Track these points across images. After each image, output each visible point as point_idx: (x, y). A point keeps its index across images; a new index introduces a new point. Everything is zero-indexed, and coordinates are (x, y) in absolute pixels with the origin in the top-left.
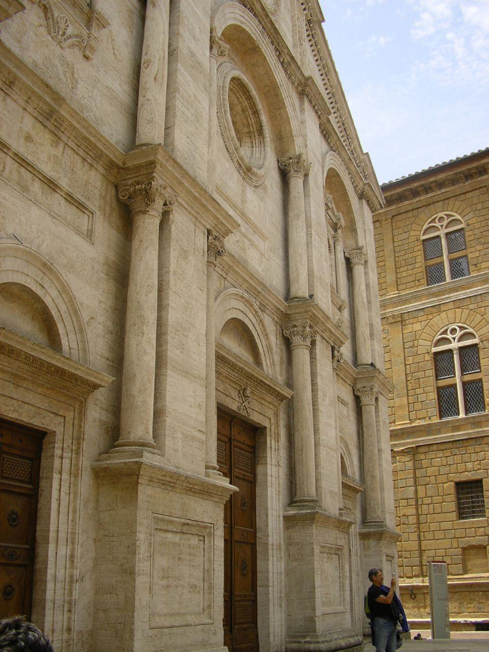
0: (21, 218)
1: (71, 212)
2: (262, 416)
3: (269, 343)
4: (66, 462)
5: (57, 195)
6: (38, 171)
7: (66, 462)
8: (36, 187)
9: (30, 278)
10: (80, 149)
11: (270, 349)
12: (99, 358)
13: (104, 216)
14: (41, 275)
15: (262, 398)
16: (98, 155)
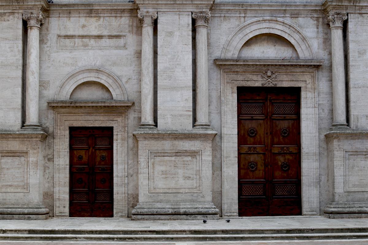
0: (85, 57)
1: (113, 42)
2: (294, 82)
3: (302, 36)
4: (119, 136)
5: (103, 39)
6: (91, 36)
7: (119, 136)
8: (92, 42)
9: (92, 77)
10: (112, 14)
11: (304, 39)
12: (134, 93)
13: (133, 34)
14: (97, 74)
15: (291, 72)
16: (123, 11)
